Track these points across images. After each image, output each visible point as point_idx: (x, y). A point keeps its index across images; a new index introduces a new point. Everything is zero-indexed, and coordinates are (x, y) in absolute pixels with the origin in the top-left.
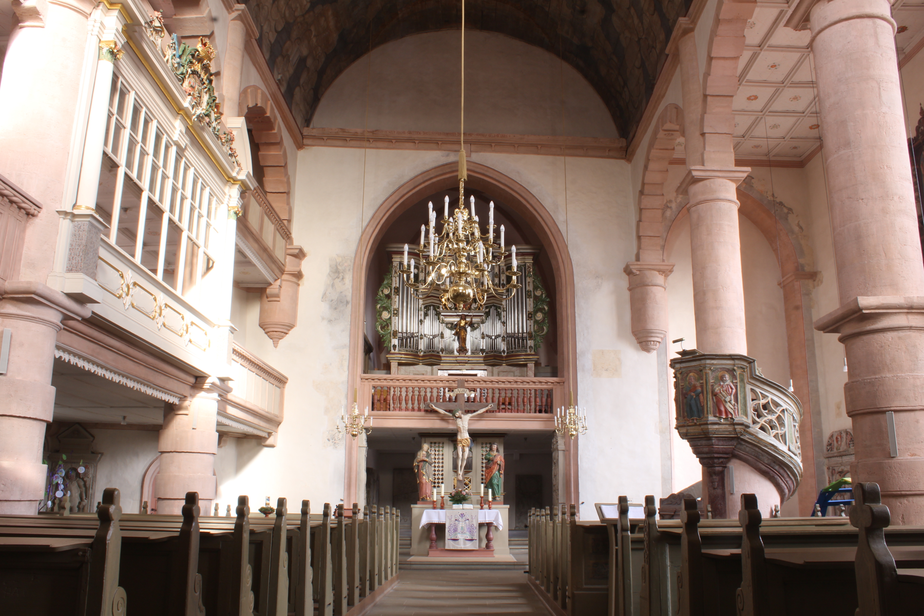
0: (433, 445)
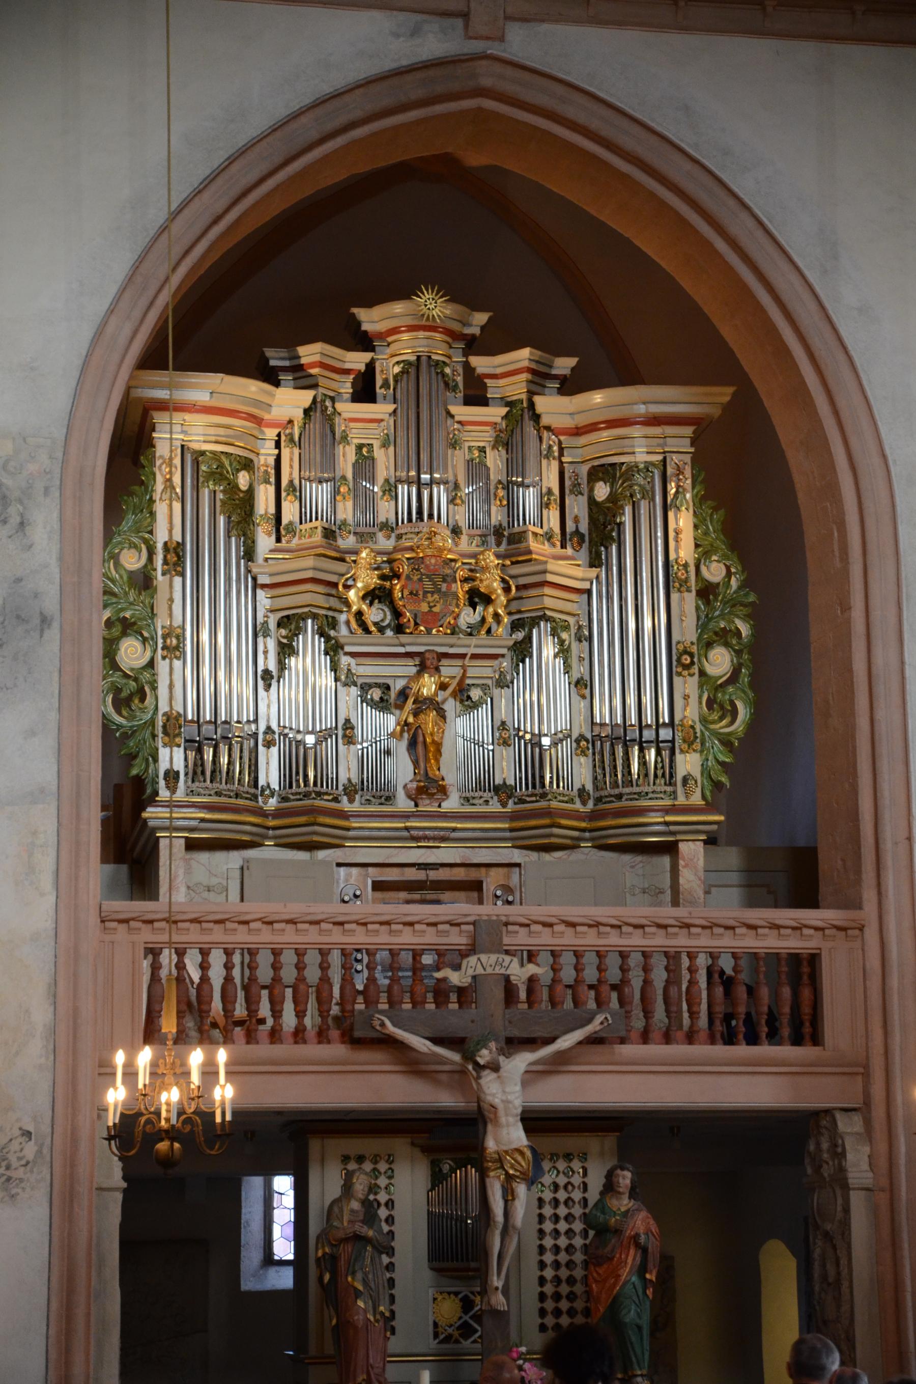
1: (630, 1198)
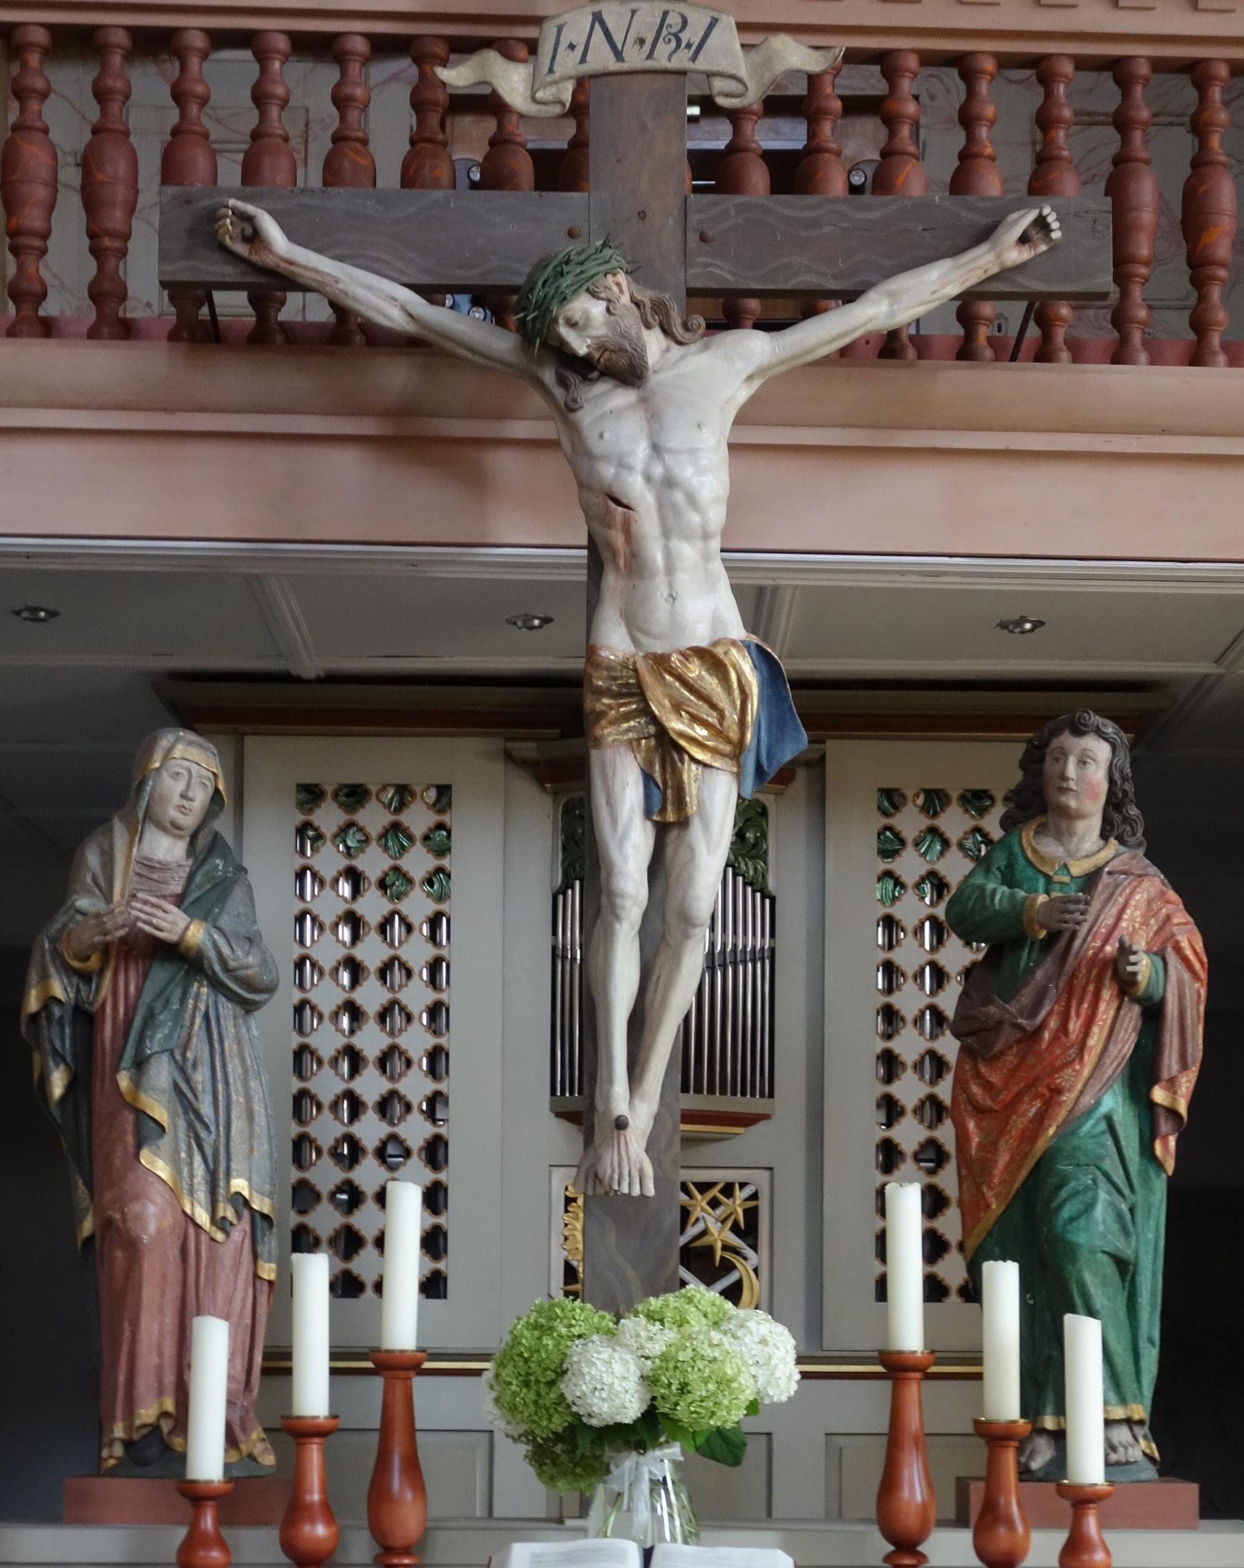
0: (328, 817)
1: (1104, 836)
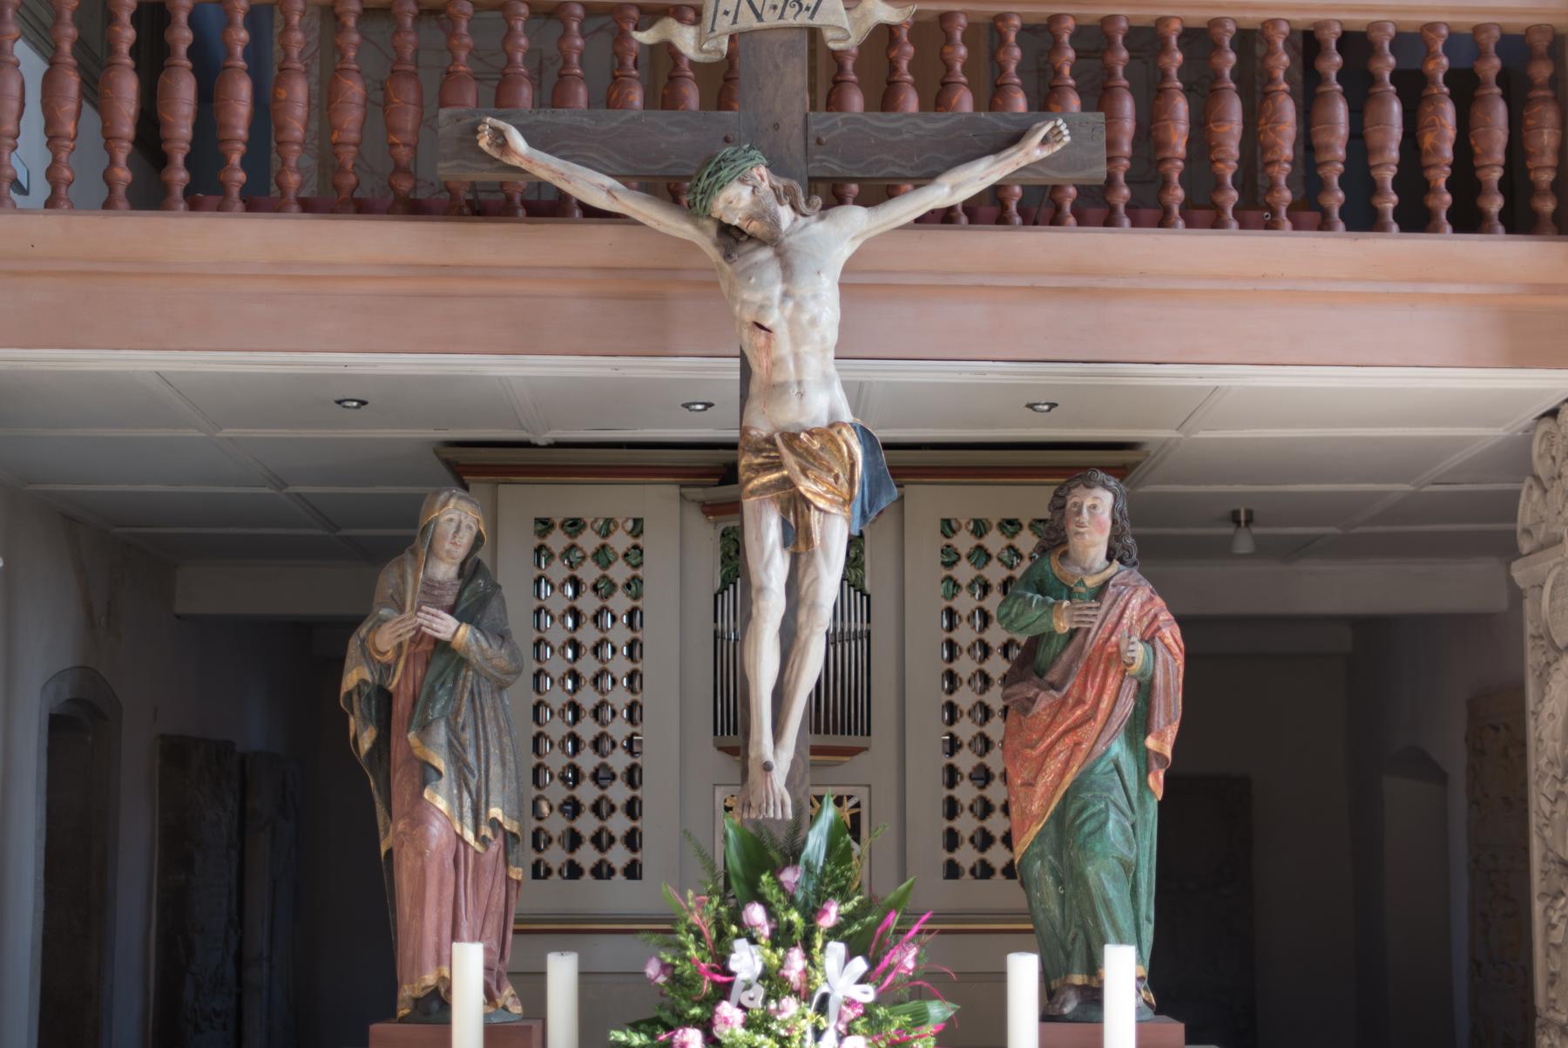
0: (557, 541)
1: (1109, 558)
